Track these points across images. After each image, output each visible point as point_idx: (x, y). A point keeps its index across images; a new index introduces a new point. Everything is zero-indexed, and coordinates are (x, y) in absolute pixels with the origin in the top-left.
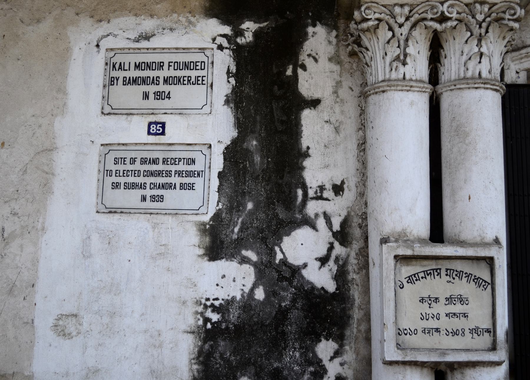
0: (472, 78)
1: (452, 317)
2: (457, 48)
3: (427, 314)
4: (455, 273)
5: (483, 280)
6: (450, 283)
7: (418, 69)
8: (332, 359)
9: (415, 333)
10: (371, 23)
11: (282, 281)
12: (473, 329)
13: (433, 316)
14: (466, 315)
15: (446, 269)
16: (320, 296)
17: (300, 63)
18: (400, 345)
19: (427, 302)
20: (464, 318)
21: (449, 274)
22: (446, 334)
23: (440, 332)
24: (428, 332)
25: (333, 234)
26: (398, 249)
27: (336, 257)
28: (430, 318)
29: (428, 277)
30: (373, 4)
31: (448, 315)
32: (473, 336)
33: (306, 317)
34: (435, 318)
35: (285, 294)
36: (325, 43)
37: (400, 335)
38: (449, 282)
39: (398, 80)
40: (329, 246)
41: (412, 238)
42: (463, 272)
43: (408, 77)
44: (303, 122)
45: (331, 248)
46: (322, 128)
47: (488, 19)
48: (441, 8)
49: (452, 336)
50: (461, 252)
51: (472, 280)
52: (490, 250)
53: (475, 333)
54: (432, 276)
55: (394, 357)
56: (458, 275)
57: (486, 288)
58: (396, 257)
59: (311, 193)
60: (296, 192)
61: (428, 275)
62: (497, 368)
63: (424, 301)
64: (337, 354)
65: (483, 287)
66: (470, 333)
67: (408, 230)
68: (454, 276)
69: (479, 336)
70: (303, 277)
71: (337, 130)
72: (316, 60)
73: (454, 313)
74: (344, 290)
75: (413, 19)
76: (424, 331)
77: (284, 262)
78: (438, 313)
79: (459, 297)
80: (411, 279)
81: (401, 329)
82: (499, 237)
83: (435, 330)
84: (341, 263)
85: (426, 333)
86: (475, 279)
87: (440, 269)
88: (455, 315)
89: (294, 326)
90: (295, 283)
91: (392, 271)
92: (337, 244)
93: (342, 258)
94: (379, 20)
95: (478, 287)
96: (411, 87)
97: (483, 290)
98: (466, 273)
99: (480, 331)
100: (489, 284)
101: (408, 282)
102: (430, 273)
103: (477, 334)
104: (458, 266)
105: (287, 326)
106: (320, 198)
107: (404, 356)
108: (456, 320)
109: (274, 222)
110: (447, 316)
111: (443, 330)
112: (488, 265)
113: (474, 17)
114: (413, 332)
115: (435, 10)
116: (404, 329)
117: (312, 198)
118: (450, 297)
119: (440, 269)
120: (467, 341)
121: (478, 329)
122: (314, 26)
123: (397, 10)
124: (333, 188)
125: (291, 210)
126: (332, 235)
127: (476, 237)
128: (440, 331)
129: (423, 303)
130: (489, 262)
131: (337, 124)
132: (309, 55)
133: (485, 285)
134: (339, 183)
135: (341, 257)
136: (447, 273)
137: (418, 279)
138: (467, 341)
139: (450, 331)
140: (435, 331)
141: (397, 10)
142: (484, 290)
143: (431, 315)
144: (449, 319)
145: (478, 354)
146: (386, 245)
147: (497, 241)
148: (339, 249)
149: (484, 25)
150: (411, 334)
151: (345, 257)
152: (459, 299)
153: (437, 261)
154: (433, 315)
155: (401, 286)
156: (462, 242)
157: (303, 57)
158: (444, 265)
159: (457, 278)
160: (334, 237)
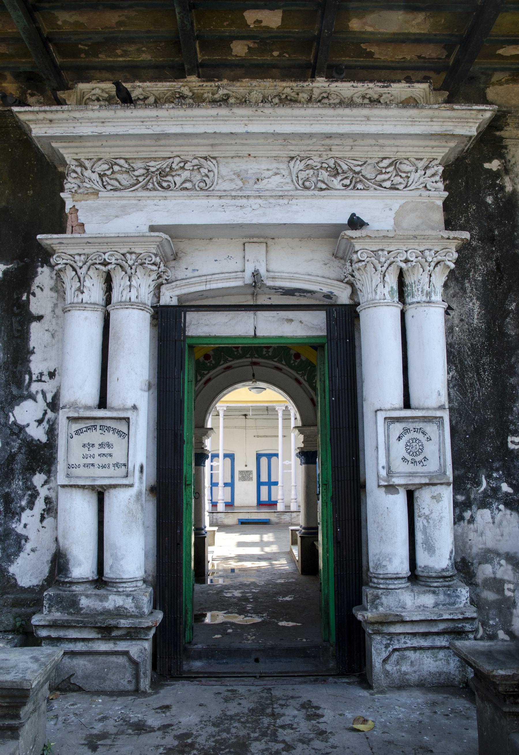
0: (125, 302)
2: (117, 282)
4: (106, 428)
7: (92, 295)
8: (43, 486)
10: (60, 266)
11: (13, 436)
16: (36, 445)
17: (32, 291)
29: (89, 431)
30: (62, 254)
33: (27, 459)
35: (15, 444)
36: (48, 278)
38: (101, 434)
39: (78, 303)
40: (44, 412)
41: (80, 406)
43: (84, 301)
44: (31, 331)
45: (45, 413)
46: (44, 334)
47: (136, 263)
48: (103, 256)
50: (114, 414)
58: (68, 418)
59: (34, 377)
60: (25, 377)
62: (130, 488)
64: (46, 482)
67: (78, 401)
70: (26, 433)
71: (53, 336)
72: (42, 290)
75: (88, 264)
77: (15, 423)
80: (77, 432)
82: (136, 405)
87: (96, 426)
89: (19, 465)
90: (21, 437)
92: (49, 411)
94: (66, 264)
96: (85, 307)
104: (108, 423)
105: (15, 465)
106: (40, 381)
108: (105, 458)
109: (10, 397)
113: (127, 262)
115: (100, 258)
117: (35, 381)
119: (96, 426)
120: (111, 472)
122: (42, 267)
123: (77, 258)
124: (49, 374)
125: (21, 388)
131: (53, 332)
132: (38, 287)
134: (52, 371)
138: (111, 472)
139: (101, 465)
141: (77, 258)
143: (89, 455)
147: (135, 407)
148: (50, 414)
149: (134, 267)
157: (34, 288)
158: (99, 423)
159: (106, 431)
160: (47, 406)
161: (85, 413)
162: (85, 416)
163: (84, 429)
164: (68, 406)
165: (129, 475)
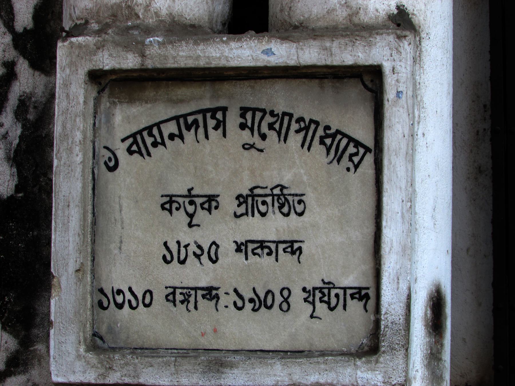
1: (254, 254)
3: (182, 245)
4: (268, 119)
5: (351, 139)
6: (253, 151)
9: (147, 301)
12: (314, 289)
13: (198, 252)
14: (296, 246)
15: (241, 108)
18: (101, 338)
19: (182, 209)
20: (289, 255)
21: (249, 124)
22: (235, 303)
23: (218, 298)
24: (182, 298)
25: (13, 40)
26: (100, 54)
27: (20, 100)
28: (191, 258)
29: (189, 136)
31: (243, 248)
32: (314, 311)
34: (205, 258)
37: (105, 309)
38: (247, 147)
41: (151, 21)
42: (291, 116)
49: (254, 310)
51: (317, 139)
52: (370, 45)
53: (321, 301)
54: (201, 130)
55: (74, 372)
56: (277, 126)
57: (360, 162)
61: (188, 128)
63: (175, 205)
65: (351, 160)
66: (306, 300)
68: (265, 129)
69: (332, 309)
73: (262, 242)
74: (36, 189)
76: (171, 297)
78: (214, 243)
79: (277, 191)
81: (106, 291)
82: (410, 9)
83: (204, 292)
84: (31, 117)
85: (177, 302)
86: (327, 136)
87: (224, 110)
88: (262, 247)
91: (78, 120)
93: (35, 102)
95: (335, 161)
97: (348, 169)
98: (300, 120)
99: (337, 296)
100: (367, 150)
101: (130, 152)
102: (196, 122)
103: (325, 306)
107: (103, 371)
108: (267, 261)
110: (238, 250)
111: (227, 293)
112: (369, 93)
114: (140, 297)
116: (115, 290)
118: (249, 193)
119: (224, 110)
121: (329, 289)
126: (11, 43)
127: (334, 10)
128: (217, 297)
129: (170, 211)
130: (370, 85)
133: (356, 154)
135: (33, 99)
136: (243, 121)
137: (159, 140)
139: (248, 295)
140: (204, 296)
142: (352, 169)
143: (193, 248)
144: (247, 259)
145: (322, 366)
146: (66, 44)
150: (134, 303)
151: (44, 100)
152: (276, 198)
153: (218, 86)
154: (199, 247)
155: (112, 164)
156: (296, 27)
159: (272, 135)
161: (170, 51)
162: (171, 64)
163: (171, 128)
164: (95, 26)
165: (384, 345)
